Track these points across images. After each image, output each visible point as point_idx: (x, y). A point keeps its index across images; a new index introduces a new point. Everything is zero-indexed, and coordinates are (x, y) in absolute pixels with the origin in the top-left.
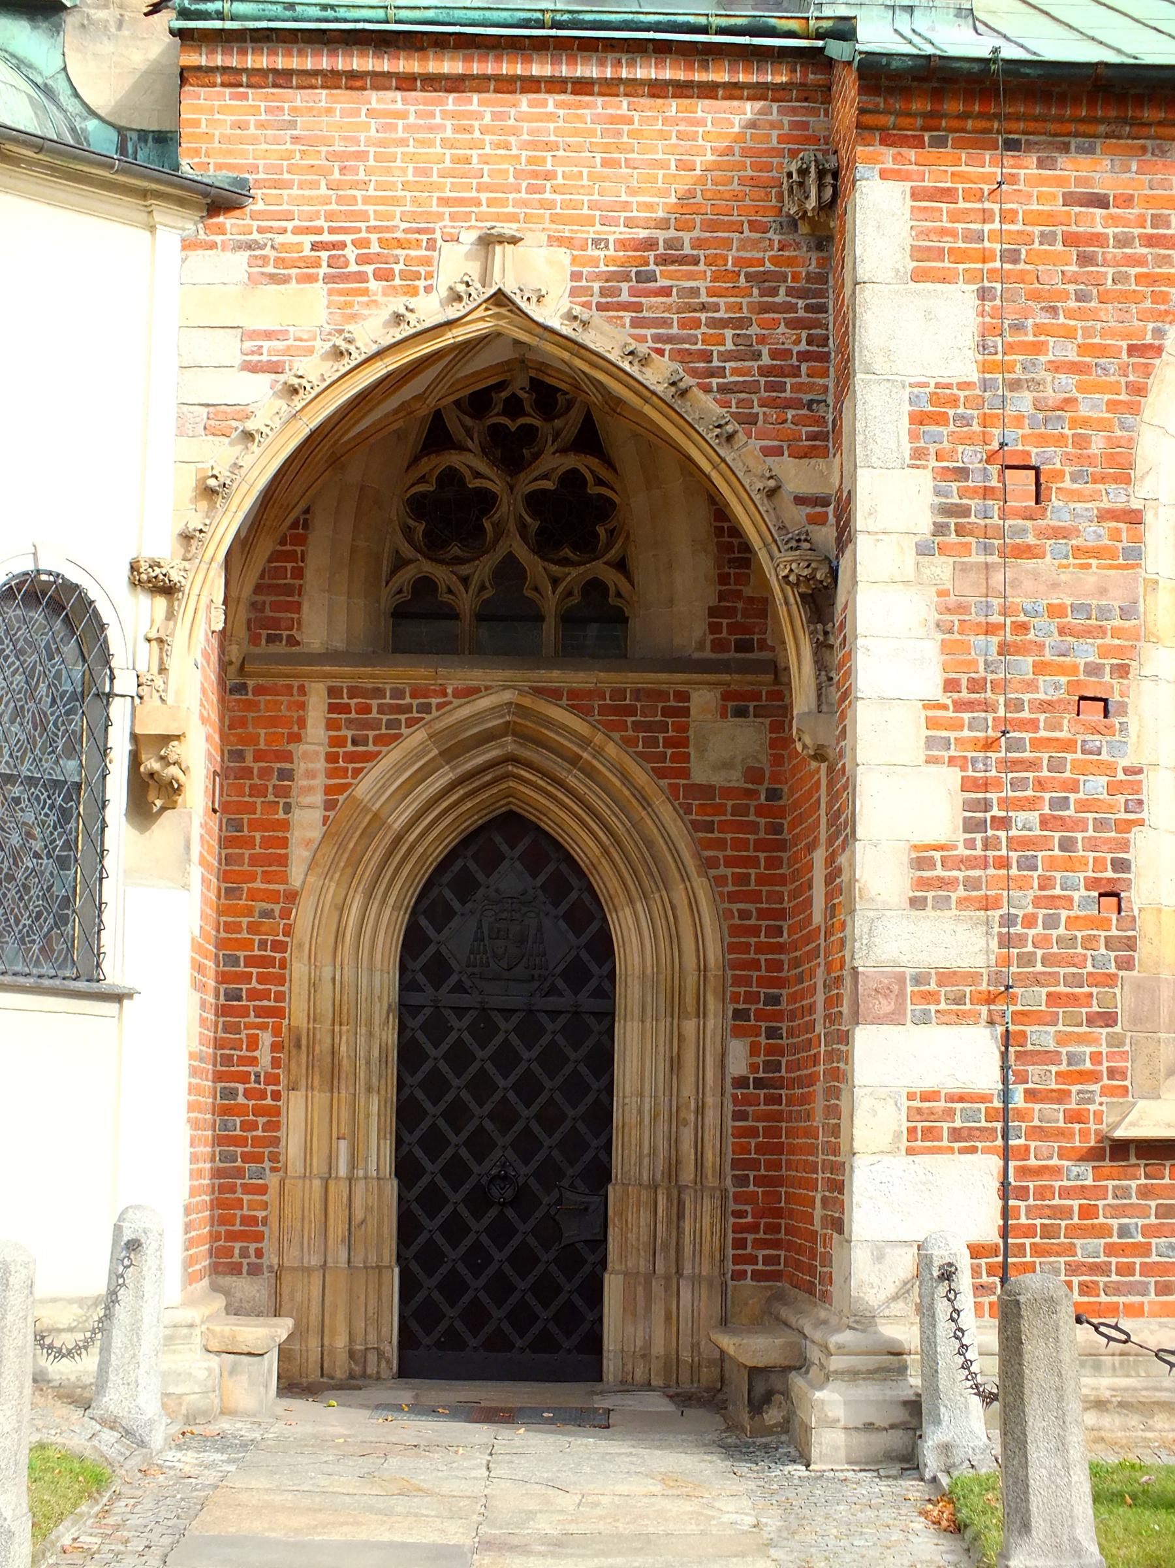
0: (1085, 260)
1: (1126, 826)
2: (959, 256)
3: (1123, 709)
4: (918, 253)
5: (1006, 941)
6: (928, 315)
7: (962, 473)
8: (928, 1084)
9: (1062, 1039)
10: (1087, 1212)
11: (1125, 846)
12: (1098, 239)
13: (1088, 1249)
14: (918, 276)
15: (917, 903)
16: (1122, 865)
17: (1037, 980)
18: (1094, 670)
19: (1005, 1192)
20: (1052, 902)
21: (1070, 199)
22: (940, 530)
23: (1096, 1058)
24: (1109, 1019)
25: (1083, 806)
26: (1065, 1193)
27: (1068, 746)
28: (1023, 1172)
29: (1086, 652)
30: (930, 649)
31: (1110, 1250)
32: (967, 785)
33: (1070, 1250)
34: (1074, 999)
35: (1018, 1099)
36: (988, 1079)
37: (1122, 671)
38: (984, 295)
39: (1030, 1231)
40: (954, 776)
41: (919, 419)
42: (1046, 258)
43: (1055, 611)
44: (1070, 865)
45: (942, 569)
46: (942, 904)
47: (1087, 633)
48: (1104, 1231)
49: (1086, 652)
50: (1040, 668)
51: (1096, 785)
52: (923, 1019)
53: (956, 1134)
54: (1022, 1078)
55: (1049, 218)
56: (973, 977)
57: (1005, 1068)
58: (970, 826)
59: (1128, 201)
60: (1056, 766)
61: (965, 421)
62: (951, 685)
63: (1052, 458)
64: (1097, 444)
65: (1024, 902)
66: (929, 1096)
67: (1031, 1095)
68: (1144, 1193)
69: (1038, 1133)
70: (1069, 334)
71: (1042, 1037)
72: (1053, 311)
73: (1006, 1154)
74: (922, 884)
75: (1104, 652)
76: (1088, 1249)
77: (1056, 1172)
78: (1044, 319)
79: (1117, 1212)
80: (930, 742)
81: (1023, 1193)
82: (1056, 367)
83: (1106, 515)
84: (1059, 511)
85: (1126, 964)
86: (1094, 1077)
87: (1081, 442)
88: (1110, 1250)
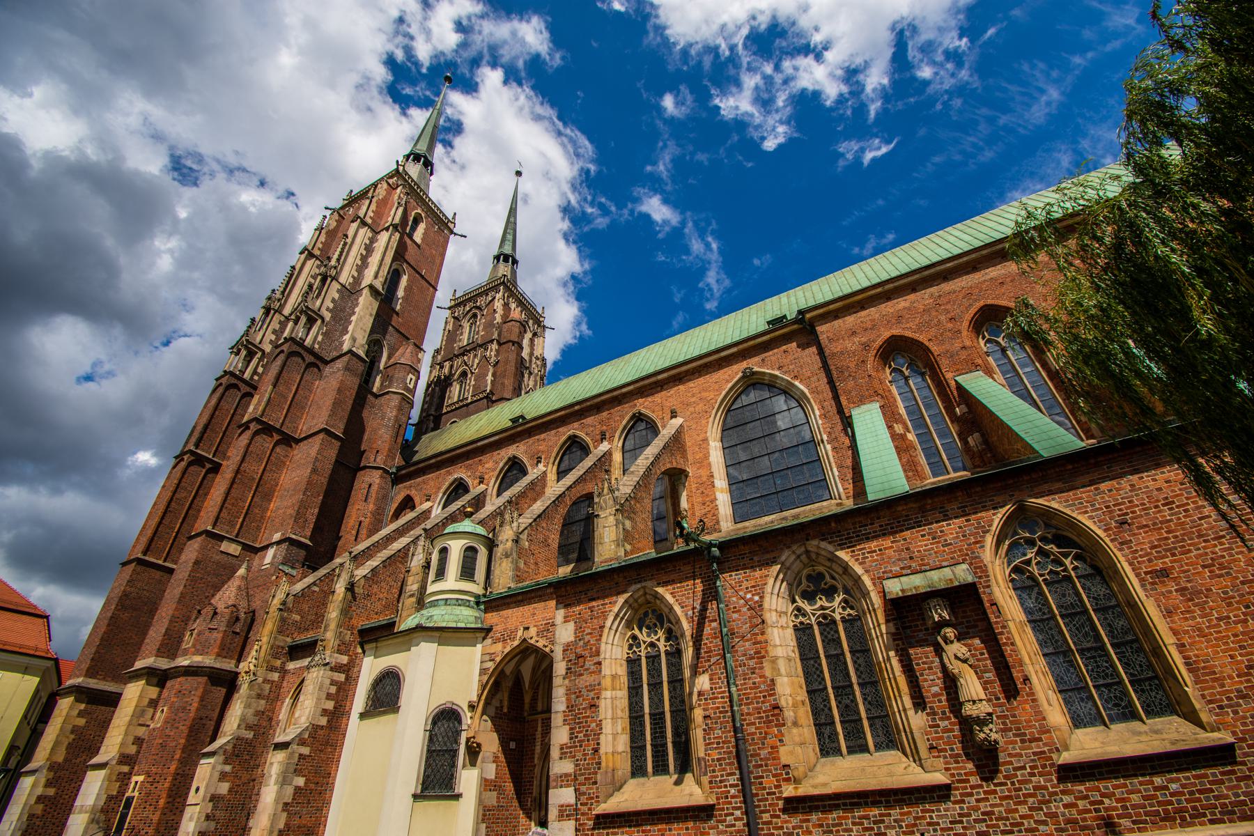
1: (599, 734)
4: (565, 617)
5: (577, 765)
8: (562, 803)
9: (587, 789)
16: (598, 744)
17: (582, 775)
18: (593, 699)
24: (595, 783)
27: (588, 717)
28: (580, 825)
29: (592, 694)
32: (571, 729)
34: (589, 779)
36: (573, 801)
37: (598, 698)
43: (586, 687)
44: (589, 745)
46: (565, 758)
49: (592, 694)
52: (561, 787)
53: (567, 816)
56: (570, 775)
58: (571, 738)
60: (586, 722)
62: (568, 707)
63: (587, 653)
64: (594, 649)
65: (579, 755)
66: (562, 806)
71: (583, 789)
73: (577, 820)
74: (562, 754)
83: (595, 664)
84: (587, 664)
86: (592, 798)
87: (591, 649)
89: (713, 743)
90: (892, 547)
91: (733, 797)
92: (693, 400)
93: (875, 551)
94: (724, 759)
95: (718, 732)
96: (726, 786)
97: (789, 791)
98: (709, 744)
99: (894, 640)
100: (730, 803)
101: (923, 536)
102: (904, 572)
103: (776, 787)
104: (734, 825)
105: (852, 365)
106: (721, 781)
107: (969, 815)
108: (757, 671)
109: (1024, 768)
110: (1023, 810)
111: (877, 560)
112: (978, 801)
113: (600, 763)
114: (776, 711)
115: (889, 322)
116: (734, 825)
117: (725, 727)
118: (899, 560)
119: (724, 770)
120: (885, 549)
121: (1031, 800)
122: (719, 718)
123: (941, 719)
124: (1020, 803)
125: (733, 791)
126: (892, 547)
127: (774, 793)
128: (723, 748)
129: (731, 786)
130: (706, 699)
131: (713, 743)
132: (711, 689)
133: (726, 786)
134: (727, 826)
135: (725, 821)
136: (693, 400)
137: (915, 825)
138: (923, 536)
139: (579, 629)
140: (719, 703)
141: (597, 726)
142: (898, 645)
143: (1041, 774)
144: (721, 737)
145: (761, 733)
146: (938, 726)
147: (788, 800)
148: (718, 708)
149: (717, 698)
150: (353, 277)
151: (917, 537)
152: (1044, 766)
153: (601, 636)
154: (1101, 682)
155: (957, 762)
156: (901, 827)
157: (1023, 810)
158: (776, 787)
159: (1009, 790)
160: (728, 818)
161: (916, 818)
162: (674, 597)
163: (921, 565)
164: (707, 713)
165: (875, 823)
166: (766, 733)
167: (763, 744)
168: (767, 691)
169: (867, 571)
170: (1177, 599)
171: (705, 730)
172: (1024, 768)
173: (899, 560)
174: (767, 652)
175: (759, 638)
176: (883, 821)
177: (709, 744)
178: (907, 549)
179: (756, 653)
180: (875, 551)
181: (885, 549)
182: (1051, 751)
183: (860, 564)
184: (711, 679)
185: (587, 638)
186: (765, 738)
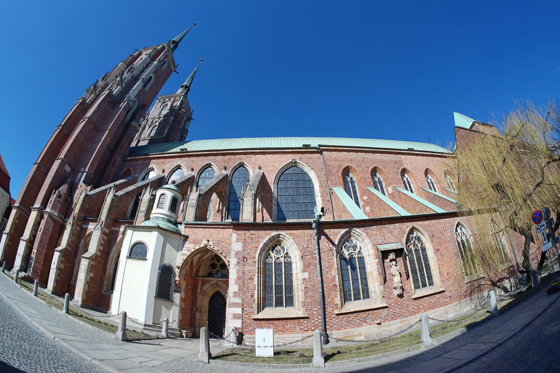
0: (252, 240)
2: (240, 240)
3: (254, 279)
4: (237, 240)
6: (237, 245)
7: (240, 259)
8: (235, 313)
10: (250, 325)
11: (254, 292)
12: (253, 238)
13: (250, 328)
14: (237, 242)
15: (234, 297)
16: (254, 294)
18: (251, 276)
19: (242, 323)
20: (247, 297)
21: (250, 234)
22: (237, 264)
23: (251, 311)
24: (252, 308)
25: (250, 288)
26: (248, 323)
27: (249, 283)
28: (244, 321)
29: (250, 274)
30: (236, 274)
31: (252, 328)
32: (239, 286)
33: (249, 328)
34: (249, 306)
35: (243, 315)
36: (241, 313)
37: (254, 276)
38: (242, 243)
39: (245, 327)
40: (238, 285)
41: (236, 254)
42: (248, 240)
43: (248, 271)
44: (248, 294)
45: (237, 267)
47: (251, 273)
48: (252, 327)
50: (246, 276)
51: (251, 286)
52: (234, 307)
54: (244, 313)
55: (249, 236)
56: (239, 303)
57: (242, 312)
59: (256, 234)
60: (248, 285)
61: (240, 254)
62: (238, 277)
63: (248, 257)
64: (252, 256)
67: (245, 314)
68: (256, 323)
69: (246, 318)
70: (250, 246)
72: (249, 244)
73: (242, 319)
75: (252, 274)
76: (250, 328)
77: (247, 321)
78: (248, 245)
79: (253, 325)
80: (236, 282)
81: (244, 323)
82: (249, 249)
84: (248, 262)
85: (254, 302)
87: (251, 255)
88: (252, 328)
89: (308, 297)
90: (379, 234)
91: (315, 314)
92: (269, 164)
93: (374, 235)
94: (313, 302)
95: (311, 293)
96: (312, 311)
97: (337, 312)
98: (307, 297)
99: (377, 265)
100: (314, 316)
101: (389, 232)
102: (382, 243)
103: (332, 311)
104: (315, 323)
105: (334, 171)
106: (310, 309)
107: (390, 313)
108: (329, 273)
109: (405, 300)
110: (403, 311)
111: (374, 238)
112: (393, 310)
113: (254, 301)
114: (335, 287)
115: (348, 161)
116: (315, 323)
117: (314, 292)
118: (381, 239)
119: (312, 306)
120: (378, 235)
121: (405, 308)
122: (312, 288)
123: (387, 288)
124: (402, 309)
125: (315, 312)
126: (379, 234)
127: (331, 313)
128: (312, 298)
129: (314, 311)
130: (306, 281)
131: (308, 297)
132: (309, 278)
133: (312, 311)
134: (311, 323)
135: (311, 322)
136: (269, 164)
137: (375, 318)
138: (389, 232)
139: (244, 246)
140: (312, 283)
141: (253, 287)
142: (378, 266)
143: (408, 301)
144: (312, 295)
145: (328, 294)
146: (386, 290)
147: (337, 315)
148: (311, 285)
149: (311, 281)
150: (138, 74)
151: (387, 232)
152: (409, 299)
153: (256, 251)
154: (422, 277)
155: (389, 300)
156: (371, 319)
157: (403, 311)
158: (332, 311)
159: (400, 306)
160: (312, 321)
161: (376, 316)
162: (294, 240)
163: (387, 241)
164: (307, 286)
165: (364, 319)
166: (330, 294)
167: (329, 297)
168: (332, 280)
169: (371, 241)
170: (440, 256)
171: (305, 292)
172: (405, 300)
173: (381, 239)
174: (333, 266)
175: (331, 261)
176: (366, 318)
177: (307, 297)
178: (384, 236)
179: (329, 266)
180: (374, 235)
181: (378, 235)
182: (411, 295)
183: (369, 239)
184: (309, 274)
185: (249, 251)
186: (330, 295)
